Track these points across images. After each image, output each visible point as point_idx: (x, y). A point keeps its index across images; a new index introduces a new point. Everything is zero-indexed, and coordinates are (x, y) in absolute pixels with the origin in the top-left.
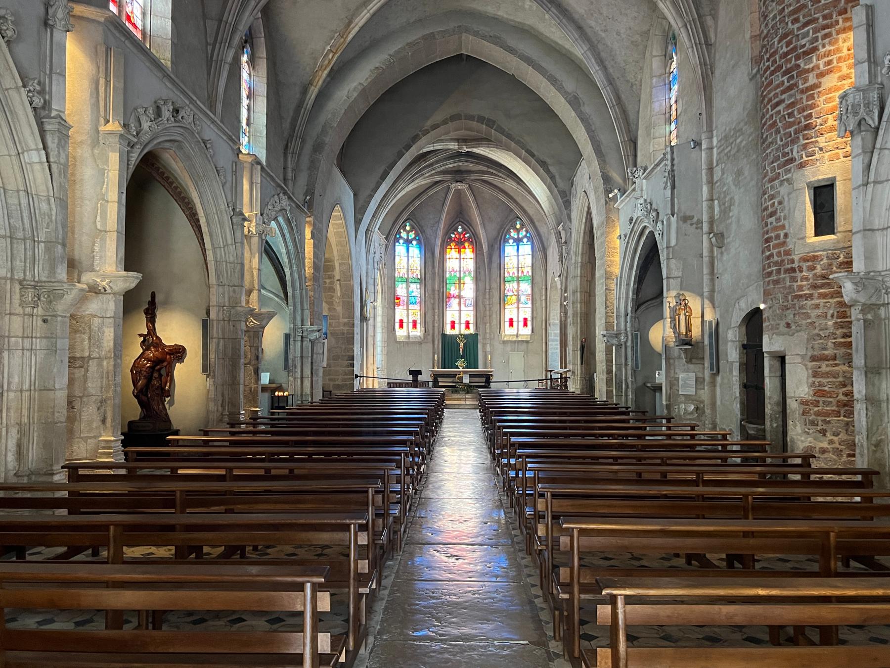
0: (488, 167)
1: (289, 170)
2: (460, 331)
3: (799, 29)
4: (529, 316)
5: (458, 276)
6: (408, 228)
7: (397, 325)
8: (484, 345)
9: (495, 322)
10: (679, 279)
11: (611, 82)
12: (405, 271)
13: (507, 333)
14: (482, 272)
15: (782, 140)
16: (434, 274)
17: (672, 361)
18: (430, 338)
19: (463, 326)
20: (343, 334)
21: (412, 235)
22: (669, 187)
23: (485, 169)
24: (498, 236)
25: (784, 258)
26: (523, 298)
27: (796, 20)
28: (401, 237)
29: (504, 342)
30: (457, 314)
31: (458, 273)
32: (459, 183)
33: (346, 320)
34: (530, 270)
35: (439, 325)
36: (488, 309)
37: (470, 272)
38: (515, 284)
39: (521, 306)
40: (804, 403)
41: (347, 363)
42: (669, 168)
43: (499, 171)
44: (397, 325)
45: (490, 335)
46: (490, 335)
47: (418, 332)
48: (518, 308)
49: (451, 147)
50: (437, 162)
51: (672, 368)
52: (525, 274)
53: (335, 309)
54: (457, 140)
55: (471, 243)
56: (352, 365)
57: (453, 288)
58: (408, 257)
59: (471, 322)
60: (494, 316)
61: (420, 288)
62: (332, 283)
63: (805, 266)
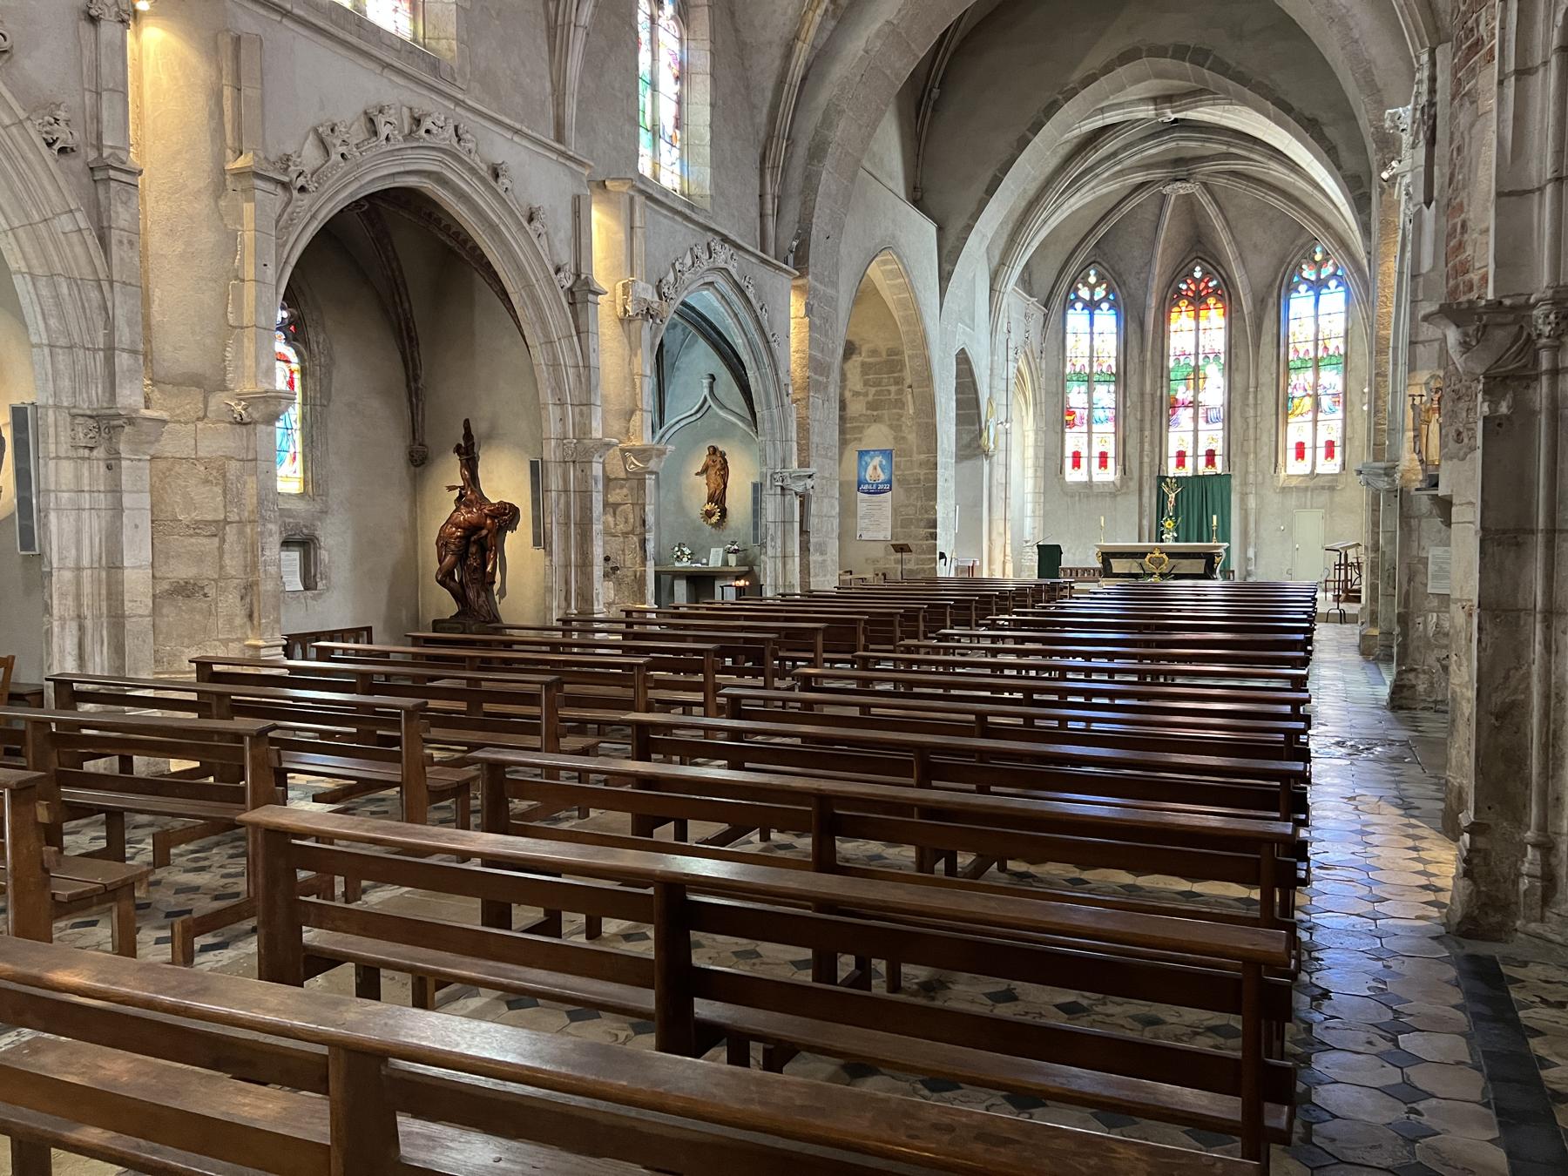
0: (1229, 144)
1: (769, 198)
2: (1195, 469)
4: (1336, 437)
5: (1193, 364)
6: (1092, 280)
7: (1069, 462)
8: (1244, 497)
9: (1266, 451)
12: (1086, 362)
13: (1290, 471)
14: (1242, 353)
16: (1143, 362)
17: (1414, 522)
18: (1134, 485)
19: (1202, 461)
20: (919, 481)
21: (1100, 293)
22: (1422, 143)
23: (1224, 148)
24: (1274, 280)
26: (1326, 402)
28: (1078, 298)
29: (1285, 490)
30: (1189, 437)
31: (1192, 357)
32: (1178, 184)
33: (923, 457)
34: (1340, 343)
35: (1152, 460)
37: (1217, 355)
38: (1309, 375)
39: (1321, 416)
41: (924, 532)
42: (1424, 99)
43: (1251, 151)
44: (1069, 462)
45: (1256, 476)
46: (1256, 476)
47: (1110, 475)
48: (1315, 421)
49: (1141, 115)
50: (1125, 148)
51: (1415, 537)
52: (1331, 353)
53: (904, 438)
54: (1155, 100)
55: (1220, 298)
56: (934, 536)
58: (1092, 333)
59: (1219, 451)
60: (1265, 439)
61: (1116, 392)
62: (900, 392)
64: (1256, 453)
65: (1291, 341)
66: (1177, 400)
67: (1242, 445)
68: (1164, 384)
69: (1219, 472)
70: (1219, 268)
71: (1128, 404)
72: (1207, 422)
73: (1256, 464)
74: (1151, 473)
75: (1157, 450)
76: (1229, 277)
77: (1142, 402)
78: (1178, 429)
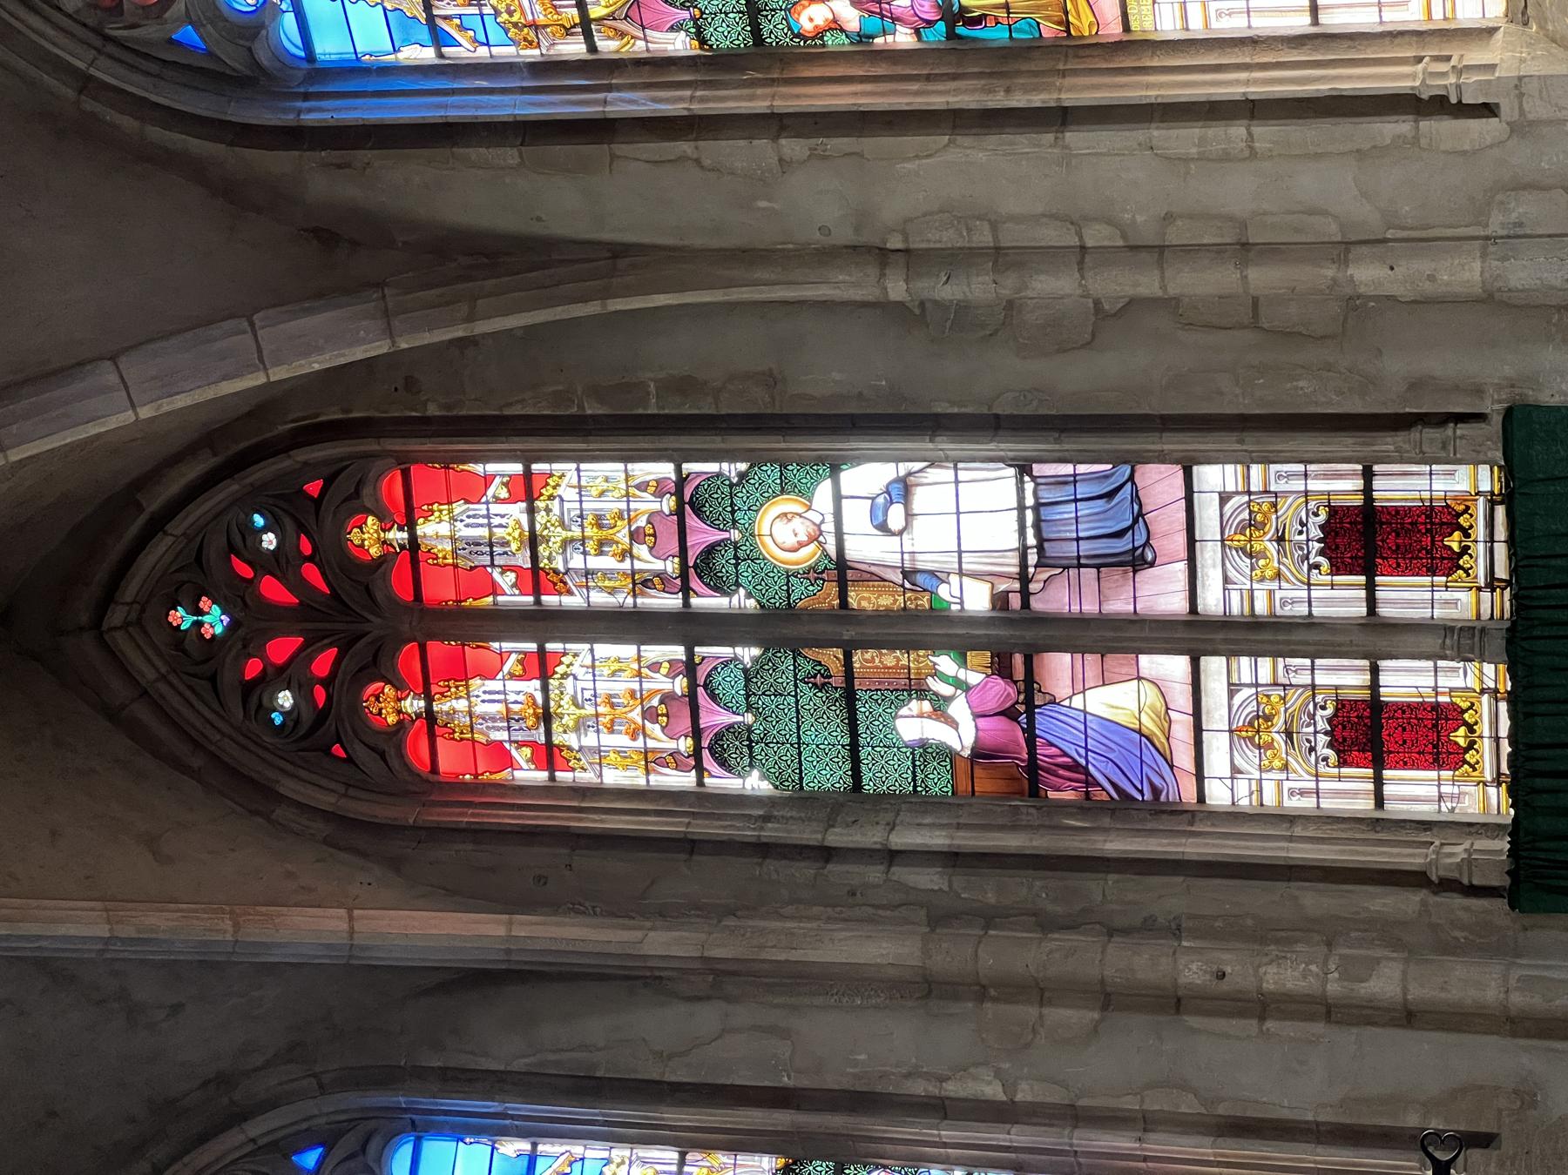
5: (748, 654)
24: (195, 170)
35: (1389, 934)
36: (1147, 284)
45: (1516, 236)
46: (1516, 236)
57: (913, 724)
64: (1344, 249)
65: (574, 48)
66: (980, 753)
67: (1288, 336)
68: (869, 836)
69: (1487, 479)
70: (155, 501)
71: (993, 1091)
72: (1137, 561)
73: (1422, 242)
74: (1483, 945)
75: (1315, 900)
76: (209, 439)
77: (981, 990)
78: (1184, 759)
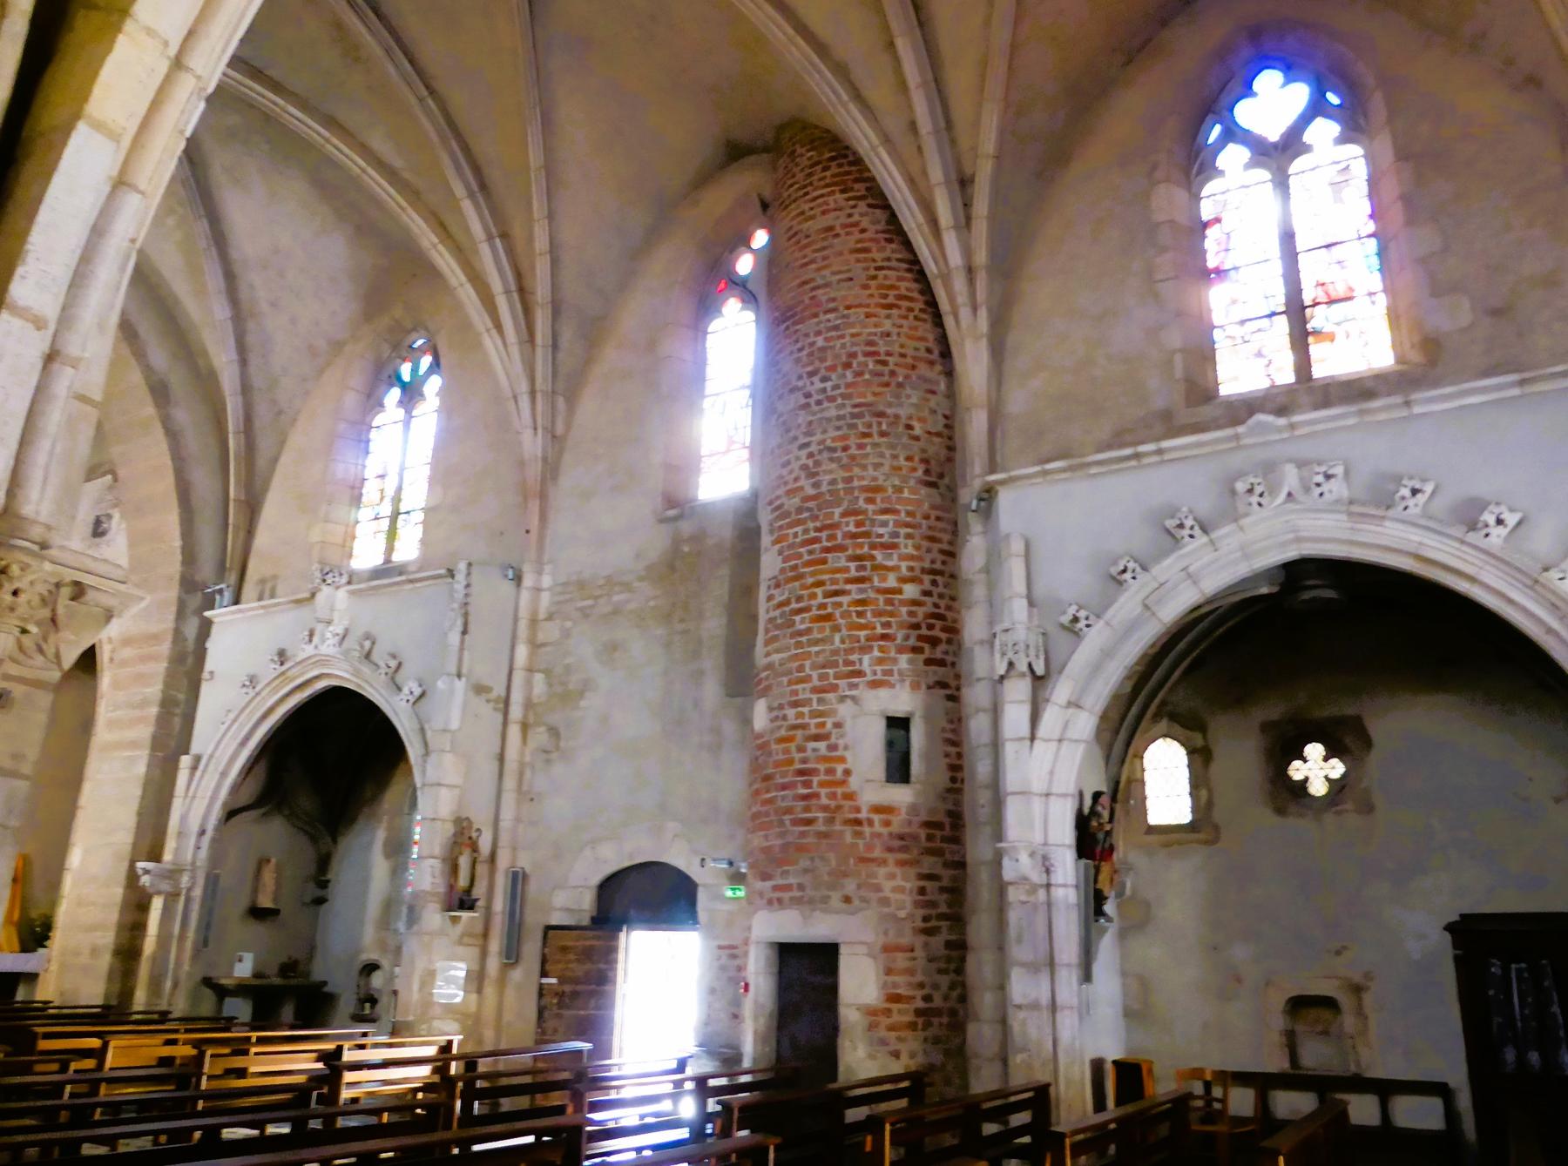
3: (875, 513)
10: (457, 791)
11: (246, 389)
15: (843, 642)
25: (843, 803)
27: (870, 501)
40: (871, 1012)
63: (876, 818)
